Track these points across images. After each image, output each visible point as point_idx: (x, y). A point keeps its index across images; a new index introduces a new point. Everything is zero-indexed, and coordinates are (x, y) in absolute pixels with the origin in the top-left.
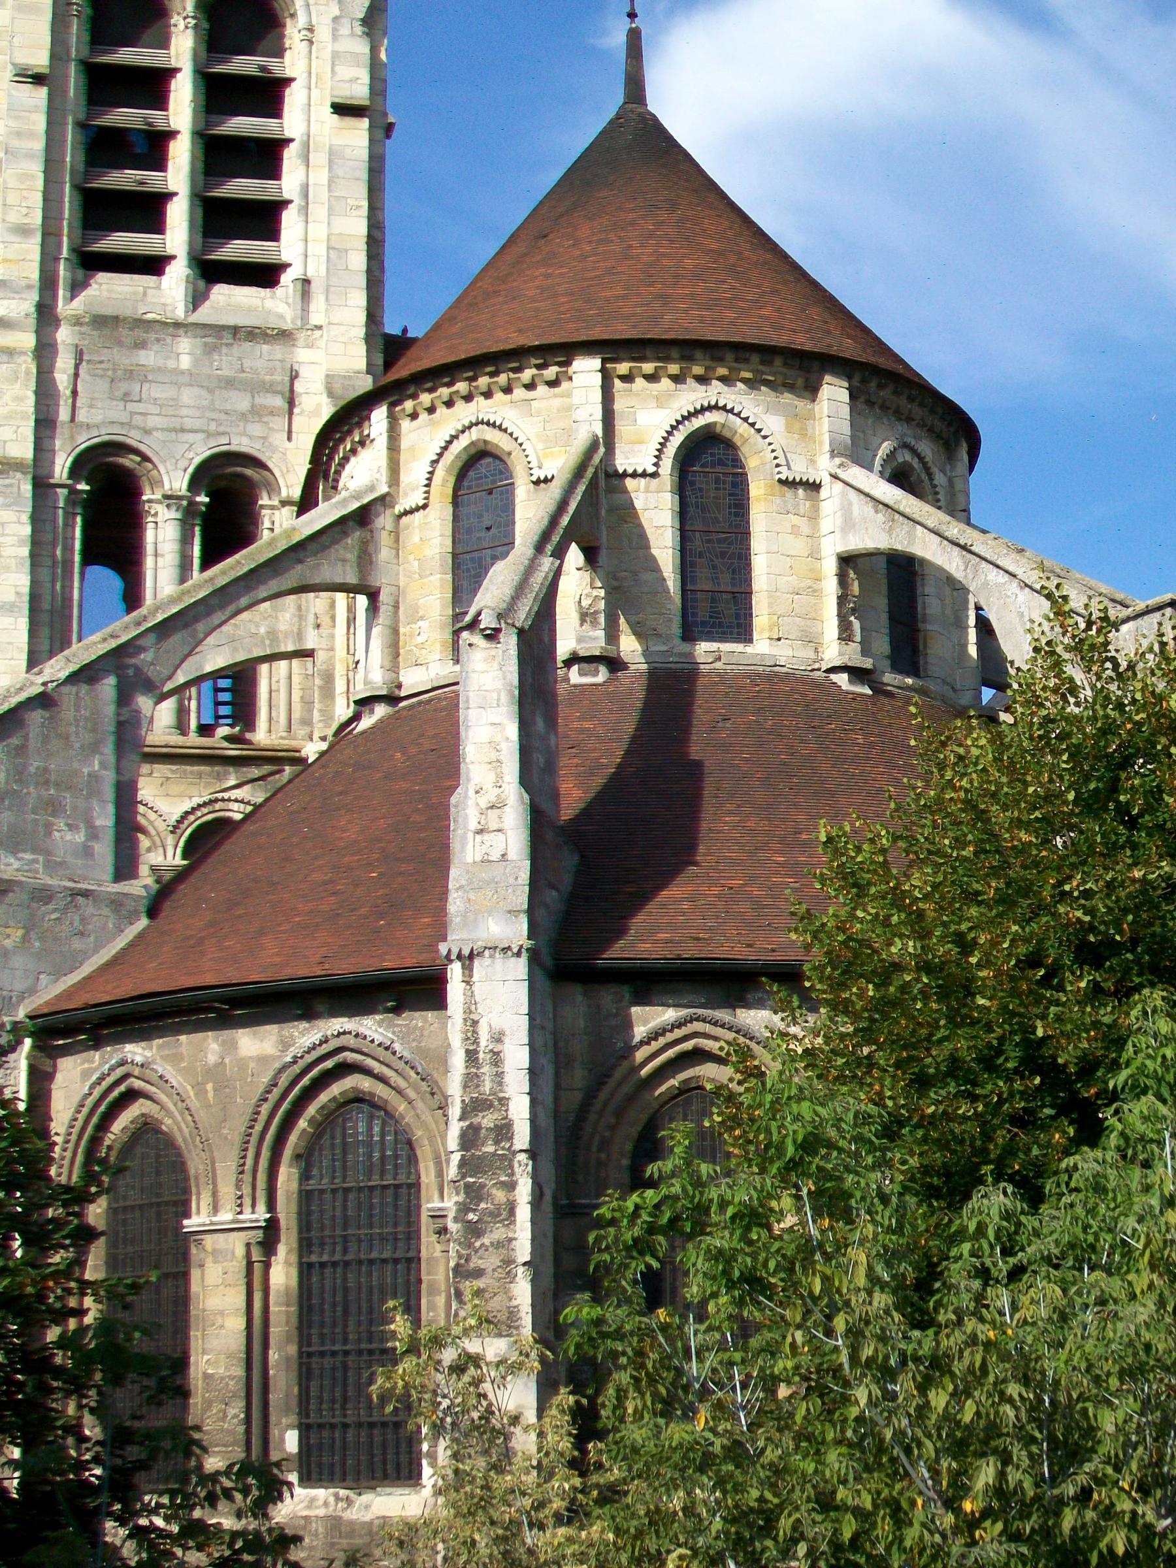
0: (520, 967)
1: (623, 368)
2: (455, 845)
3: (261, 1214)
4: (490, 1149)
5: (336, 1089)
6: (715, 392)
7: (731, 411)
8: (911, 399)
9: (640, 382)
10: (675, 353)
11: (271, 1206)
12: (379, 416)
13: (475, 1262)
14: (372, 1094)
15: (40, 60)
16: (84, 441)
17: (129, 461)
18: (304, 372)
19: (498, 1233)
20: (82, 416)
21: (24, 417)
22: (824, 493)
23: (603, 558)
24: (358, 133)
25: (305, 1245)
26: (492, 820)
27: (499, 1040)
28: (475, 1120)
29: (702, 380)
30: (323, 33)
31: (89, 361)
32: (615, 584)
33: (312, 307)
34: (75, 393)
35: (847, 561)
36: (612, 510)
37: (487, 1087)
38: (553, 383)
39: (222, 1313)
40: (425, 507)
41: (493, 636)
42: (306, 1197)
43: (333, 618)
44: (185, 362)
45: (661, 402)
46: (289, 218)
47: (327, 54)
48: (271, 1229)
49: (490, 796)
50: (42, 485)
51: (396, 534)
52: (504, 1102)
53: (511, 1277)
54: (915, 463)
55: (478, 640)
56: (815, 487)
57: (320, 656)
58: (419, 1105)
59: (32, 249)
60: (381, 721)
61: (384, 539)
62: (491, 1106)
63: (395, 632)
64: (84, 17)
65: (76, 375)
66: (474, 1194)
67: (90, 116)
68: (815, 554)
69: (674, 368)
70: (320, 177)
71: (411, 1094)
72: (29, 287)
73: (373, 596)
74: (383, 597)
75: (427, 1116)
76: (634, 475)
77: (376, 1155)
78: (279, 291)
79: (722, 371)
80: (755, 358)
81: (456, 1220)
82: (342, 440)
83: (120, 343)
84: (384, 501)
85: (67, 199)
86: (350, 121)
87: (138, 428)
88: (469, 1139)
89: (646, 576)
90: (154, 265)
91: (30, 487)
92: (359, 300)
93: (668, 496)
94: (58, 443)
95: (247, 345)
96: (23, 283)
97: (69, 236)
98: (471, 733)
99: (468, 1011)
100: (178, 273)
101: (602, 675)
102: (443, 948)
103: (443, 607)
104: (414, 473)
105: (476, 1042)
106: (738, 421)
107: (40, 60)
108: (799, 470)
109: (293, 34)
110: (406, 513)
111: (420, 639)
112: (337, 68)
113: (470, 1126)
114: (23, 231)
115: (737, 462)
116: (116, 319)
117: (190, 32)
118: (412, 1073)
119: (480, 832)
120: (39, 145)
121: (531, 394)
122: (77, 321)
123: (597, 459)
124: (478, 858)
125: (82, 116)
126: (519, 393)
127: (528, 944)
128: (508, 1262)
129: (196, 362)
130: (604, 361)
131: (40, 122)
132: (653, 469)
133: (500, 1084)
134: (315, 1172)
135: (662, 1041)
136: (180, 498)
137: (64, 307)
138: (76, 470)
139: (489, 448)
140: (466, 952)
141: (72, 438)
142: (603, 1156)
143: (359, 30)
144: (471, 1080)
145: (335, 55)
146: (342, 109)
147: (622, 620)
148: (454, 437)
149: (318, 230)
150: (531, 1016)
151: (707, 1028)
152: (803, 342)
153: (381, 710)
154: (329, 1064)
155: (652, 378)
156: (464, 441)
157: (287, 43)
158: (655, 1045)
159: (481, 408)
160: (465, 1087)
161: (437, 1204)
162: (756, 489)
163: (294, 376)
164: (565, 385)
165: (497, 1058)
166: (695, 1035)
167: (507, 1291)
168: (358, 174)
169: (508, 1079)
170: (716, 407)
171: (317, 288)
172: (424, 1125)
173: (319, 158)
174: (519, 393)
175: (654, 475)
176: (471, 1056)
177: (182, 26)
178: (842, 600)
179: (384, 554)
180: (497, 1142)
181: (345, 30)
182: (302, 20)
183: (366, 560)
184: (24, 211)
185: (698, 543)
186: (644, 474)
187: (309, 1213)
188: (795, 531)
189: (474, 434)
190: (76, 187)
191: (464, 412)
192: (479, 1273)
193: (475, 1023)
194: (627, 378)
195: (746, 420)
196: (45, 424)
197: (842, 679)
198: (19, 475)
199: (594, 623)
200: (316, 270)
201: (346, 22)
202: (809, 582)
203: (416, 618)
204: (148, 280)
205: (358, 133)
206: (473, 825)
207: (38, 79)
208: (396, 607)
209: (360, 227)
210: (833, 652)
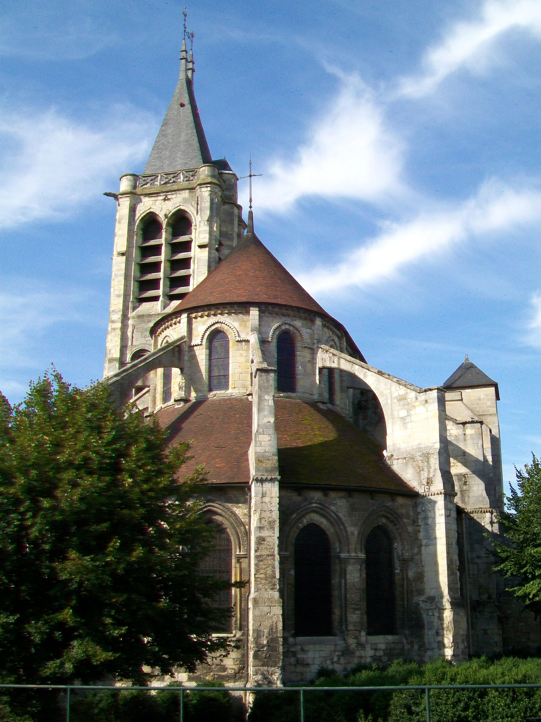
1: (193, 315)
6: (219, 318)
7: (222, 323)
8: (287, 310)
9: (199, 318)
10: (206, 309)
16: (135, 350)
20: (134, 343)
21: (118, 346)
23: (185, 370)
29: (215, 315)
31: (136, 328)
32: (191, 377)
34: (133, 337)
45: (204, 323)
54: (291, 328)
59: (121, 300)
64: (139, 235)
65: (133, 332)
67: (142, 260)
69: (206, 313)
72: (120, 311)
76: (196, 345)
79: (219, 312)
80: (228, 306)
83: (144, 322)
85: (132, 285)
86: (203, 249)
87: (148, 344)
89: (198, 374)
90: (155, 299)
91: (118, 365)
93: (204, 350)
94: (128, 352)
96: (118, 310)
97: (133, 295)
101: (182, 404)
103: (161, 389)
106: (225, 325)
108: (243, 337)
112: (200, 235)
114: (118, 296)
115: (227, 337)
116: (143, 315)
120: (123, 272)
122: (134, 318)
125: (139, 260)
126: (174, 326)
131: (123, 266)
132: (201, 343)
137: (131, 314)
141: (131, 350)
143: (206, 223)
147: (192, 388)
152: (244, 299)
155: (202, 317)
168: (205, 264)
170: (218, 322)
175: (201, 345)
181: (202, 224)
182: (194, 223)
184: (119, 290)
186: (198, 345)
188: (241, 355)
190: (135, 280)
194: (196, 318)
195: (226, 325)
196: (123, 348)
198: (115, 362)
199: (182, 390)
201: (203, 222)
202: (245, 370)
207: (123, 254)
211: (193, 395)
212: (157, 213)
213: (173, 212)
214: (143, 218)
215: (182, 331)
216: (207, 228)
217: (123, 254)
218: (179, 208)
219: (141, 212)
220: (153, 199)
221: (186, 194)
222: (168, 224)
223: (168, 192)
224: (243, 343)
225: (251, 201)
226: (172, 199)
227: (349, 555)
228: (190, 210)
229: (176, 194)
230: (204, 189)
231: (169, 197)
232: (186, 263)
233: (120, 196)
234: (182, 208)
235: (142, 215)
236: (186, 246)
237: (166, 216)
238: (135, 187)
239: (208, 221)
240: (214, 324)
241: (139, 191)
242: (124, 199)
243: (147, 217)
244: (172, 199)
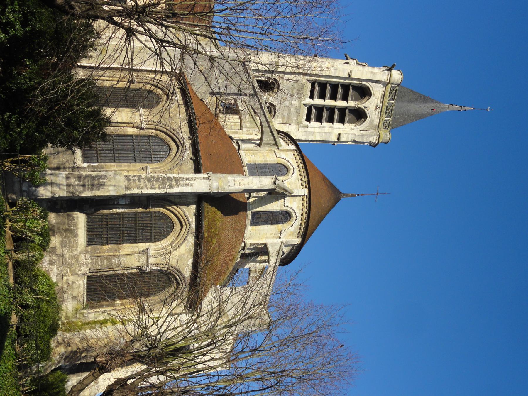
0: (206, 190)
1: (305, 199)
2: (231, 175)
3: (144, 126)
4: (167, 183)
5: (173, 144)
11: (146, 128)
12: (293, 147)
13: (142, 180)
14: (172, 153)
15: (353, 76)
16: (281, 81)
17: (276, 90)
18: (290, 126)
19: (149, 185)
22: (278, 239)
24: (334, 138)
25: (137, 136)
26: (237, 183)
27: (191, 185)
28: (173, 180)
30: (352, 132)
33: (302, 128)
35: (265, 245)
36: (278, 197)
37: (181, 183)
38: (302, 185)
39: (121, 116)
40: (277, 157)
41: (274, 183)
42: (149, 137)
43: (248, 134)
44: (294, 102)
45: (298, 207)
46: (319, 124)
47: (348, 133)
48: (142, 129)
49: (242, 183)
50: (272, 72)
51: (271, 151)
52: (178, 186)
53: (139, 188)
55: (273, 180)
56: (280, 238)
57: (241, 131)
58: (171, 164)
60: (235, 147)
61: (270, 148)
62: (177, 184)
63: (252, 150)
66: (157, 180)
68: (267, 238)
70: (326, 130)
71: (173, 162)
73: (259, 145)
74: (259, 148)
75: (168, 166)
77: (158, 153)
78: (305, 121)
81: (151, 176)
82: (287, 138)
84: (278, 148)
88: (169, 179)
90: (312, 97)
92: (304, 138)
95: (296, 115)
98: (254, 178)
99: (197, 178)
100: (309, 101)
102: (211, 173)
104: (283, 155)
105: (191, 180)
107: (353, 76)
108: (283, 234)
109: (352, 126)
110: (275, 153)
111: (250, 155)
113: (172, 179)
117: (355, 106)
118: (178, 162)
119: (234, 181)
121: (300, 180)
123: (287, 193)
124: (229, 180)
127: (212, 192)
128: (142, 188)
129: (294, 105)
130: (306, 196)
133: (182, 186)
134: (153, 138)
135: (185, 218)
136: (268, 101)
138: (275, 79)
139: (289, 171)
140: (210, 178)
142: (160, 206)
143: (353, 139)
144: (182, 179)
145: (349, 134)
146: (339, 135)
148: (291, 164)
149: (316, 130)
150: (197, 192)
151: (188, 228)
153: (237, 147)
154: (179, 143)
156: (290, 166)
157: (350, 124)
158: (184, 217)
159: (297, 169)
160: (181, 178)
161: (149, 168)
162: (280, 226)
163: (290, 124)
164: (301, 187)
165: (187, 185)
166: (186, 225)
167: (135, 188)
169: (182, 187)
171: (306, 129)
172: (166, 165)
173: (330, 130)
174: (300, 177)
175: (284, 206)
176: (188, 179)
177: (356, 104)
178: (258, 244)
179: (267, 148)
180: (169, 185)
183: (268, 144)
185: (270, 214)
186: (284, 203)
187: (144, 137)
188: (271, 234)
189: (292, 168)
190: (328, 81)
191: (296, 166)
192: (139, 181)
193: (195, 180)
194: (303, 200)
197: (243, 245)
200: (309, 129)
203: (255, 154)
204: (309, 96)
205: (334, 138)
206: (236, 179)
207: (349, 75)
208: (257, 150)
209: (317, 139)
210: (249, 242)
211: (251, 200)
214: (368, 87)
215: (296, 191)
216: (350, 140)
217: (349, 75)
218: (368, 117)
219: (373, 88)
220: (380, 98)
221: (376, 122)
222: (359, 108)
223: (381, 109)
224: (279, 235)
225: (362, 195)
230: (375, 137)
231: (377, 110)
232: (331, 120)
233: (390, 74)
234: (368, 119)
235: (371, 89)
236: (342, 121)
237: (365, 107)
241: (389, 86)
242: (386, 77)
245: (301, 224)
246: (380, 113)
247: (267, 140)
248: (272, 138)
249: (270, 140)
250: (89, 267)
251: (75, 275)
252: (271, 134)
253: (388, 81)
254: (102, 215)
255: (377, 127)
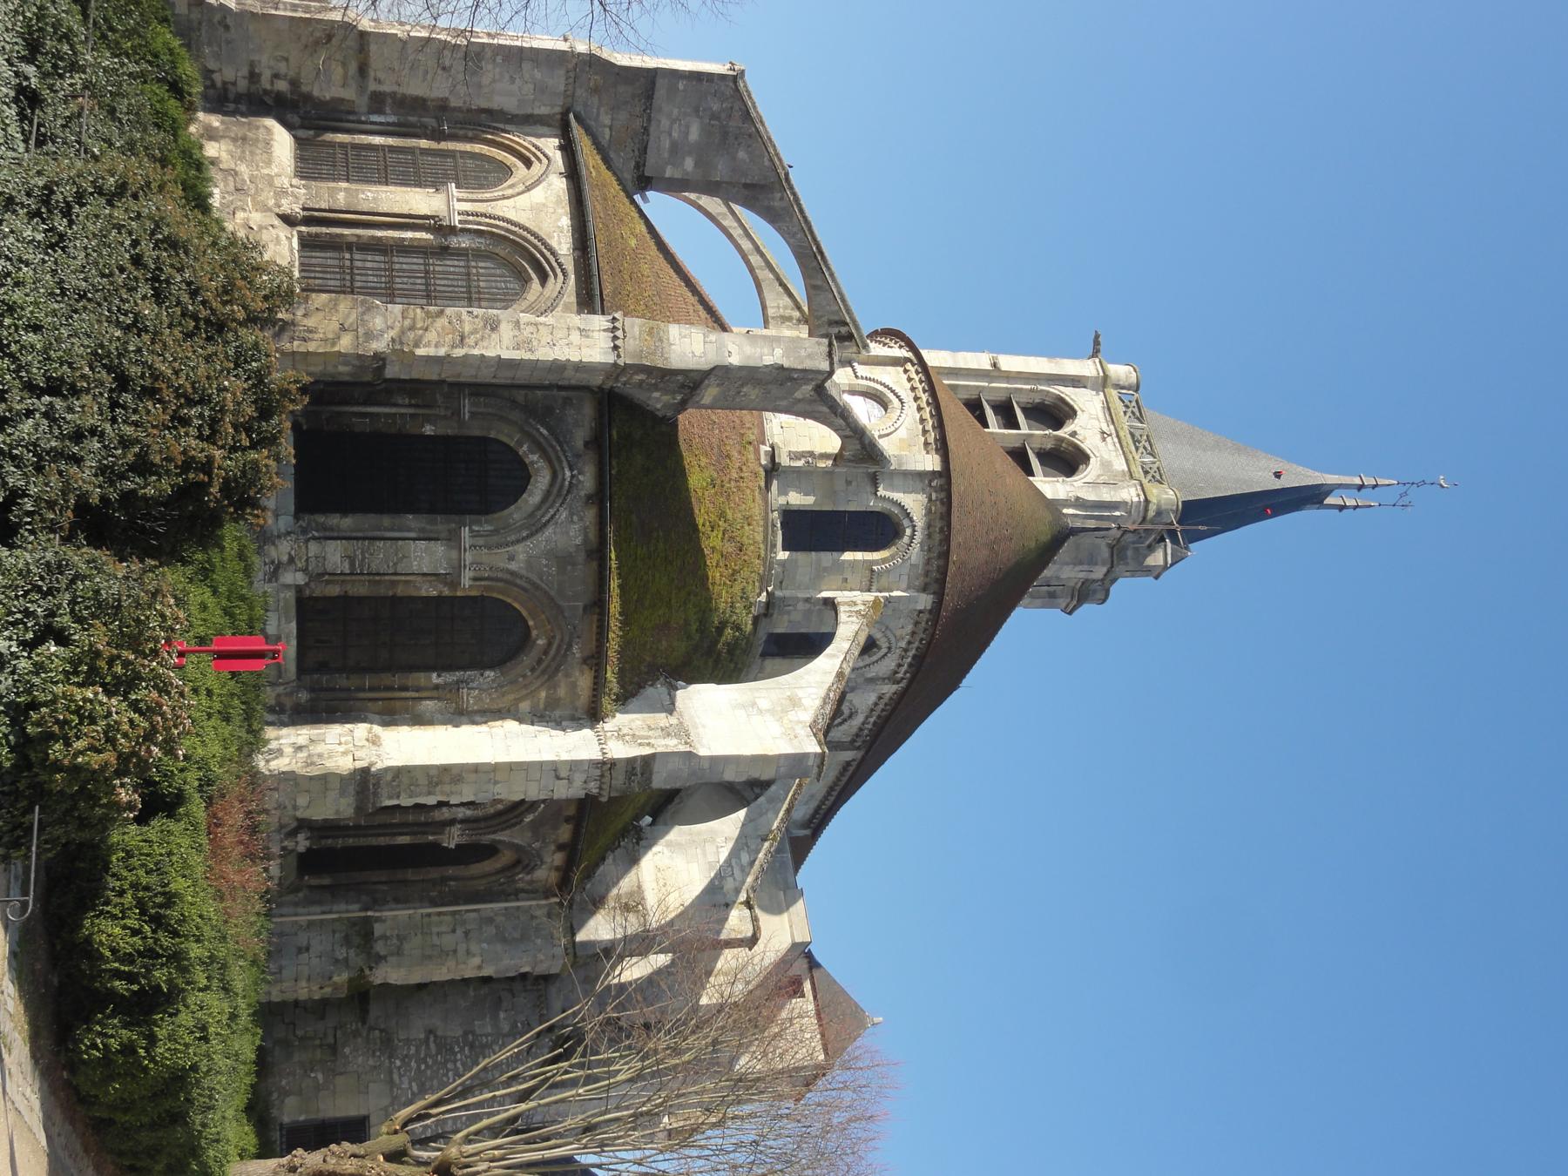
8: (941, 530)
54: (906, 539)
64: (1032, 395)
93: (847, 382)
152: (951, 445)
175: (857, 377)
186: (855, 373)
194: (906, 371)
207: (995, 365)
212: (1076, 421)
213: (1082, 445)
218: (1091, 455)
220: (1101, 415)
223: (1118, 436)
226: (1106, 444)
227: (467, 546)
228: (1091, 472)
229: (1116, 450)
231: (1109, 439)
237: (1074, 434)
238: (1118, 386)
239: (1078, 498)
240: (898, 397)
243: (1067, 409)
244: (1106, 444)
245: (922, 421)
246: (1118, 445)
247: (778, 307)
248: (787, 300)
249: (785, 308)
250: (301, 202)
251: (265, 211)
252: (780, 289)
253: (1101, 374)
254: (332, 144)
255: (1128, 475)
